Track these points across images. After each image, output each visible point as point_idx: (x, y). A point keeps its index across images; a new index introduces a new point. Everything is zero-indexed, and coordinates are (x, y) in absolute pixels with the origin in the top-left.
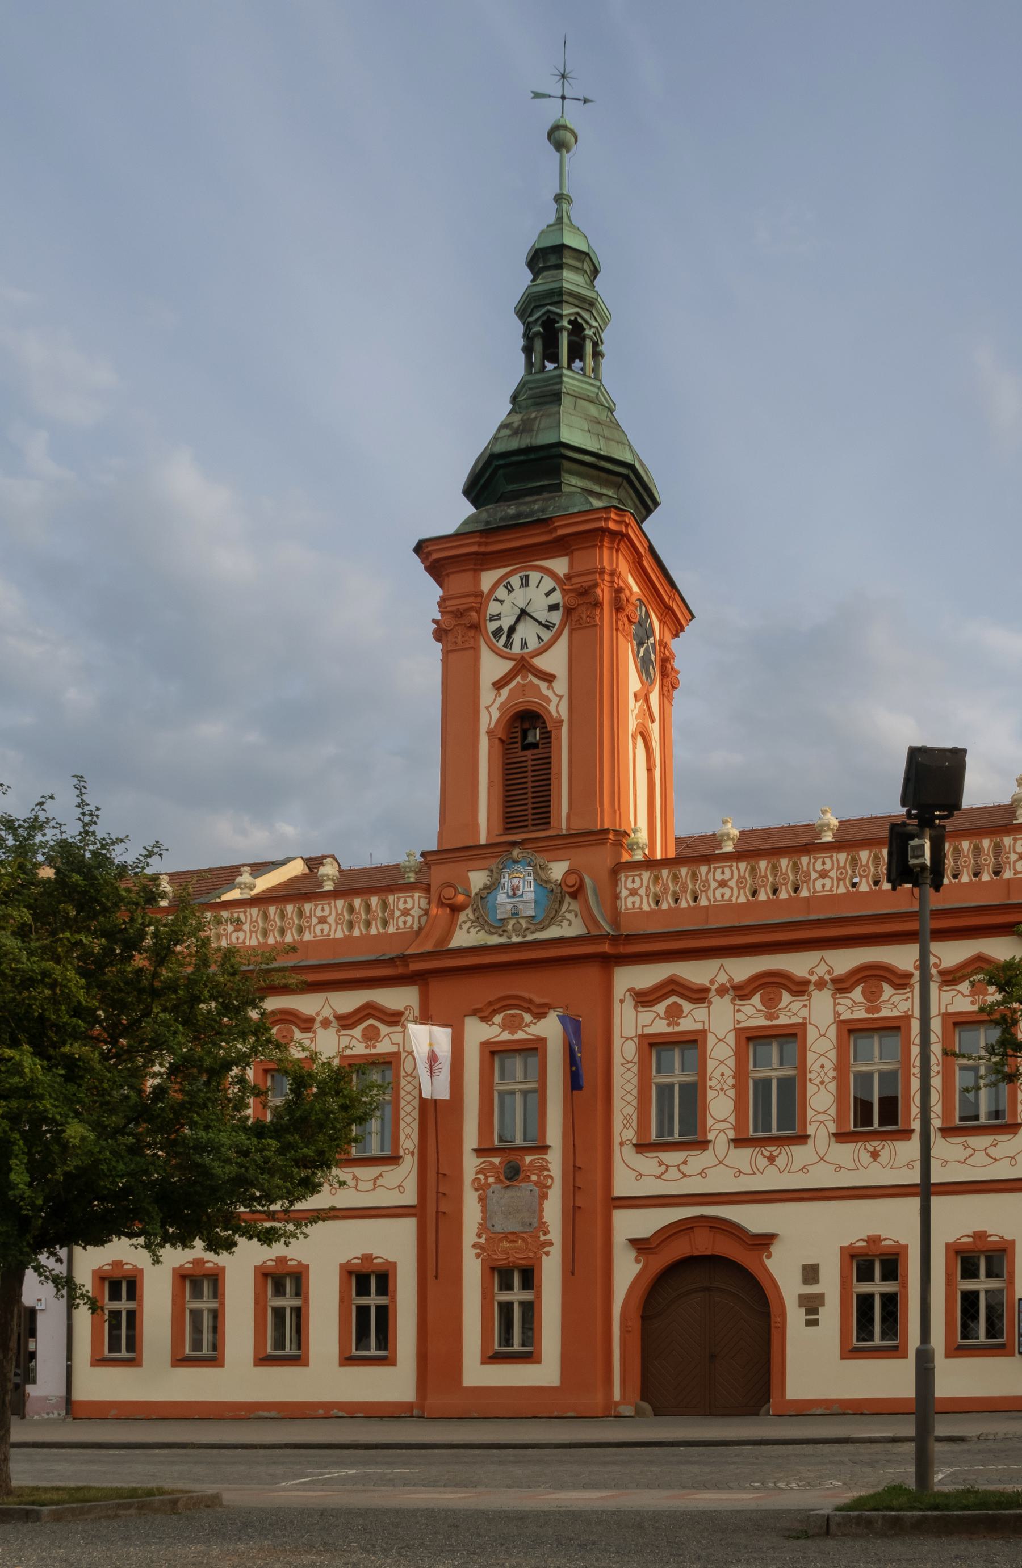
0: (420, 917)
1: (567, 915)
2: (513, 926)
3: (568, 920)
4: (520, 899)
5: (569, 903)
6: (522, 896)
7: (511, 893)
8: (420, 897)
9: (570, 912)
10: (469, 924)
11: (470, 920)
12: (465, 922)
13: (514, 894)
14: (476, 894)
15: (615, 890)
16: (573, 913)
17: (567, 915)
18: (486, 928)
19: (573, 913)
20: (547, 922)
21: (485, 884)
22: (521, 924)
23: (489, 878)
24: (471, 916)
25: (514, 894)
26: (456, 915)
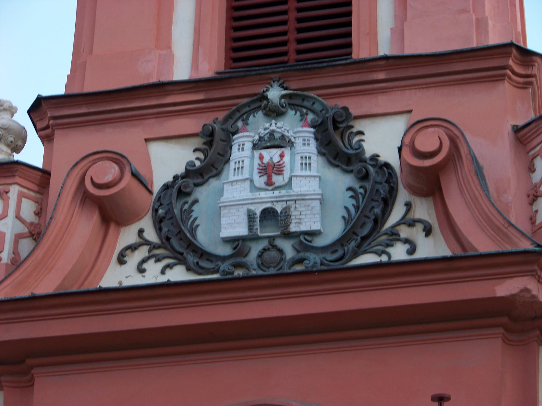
0: (18, 237)
1: (404, 232)
2: (260, 256)
3: (406, 241)
4: (283, 192)
5: (408, 205)
6: (289, 185)
7: (259, 181)
8: (21, 196)
9: (412, 224)
10: (143, 252)
11: (147, 243)
12: (133, 248)
13: (269, 183)
14: (166, 187)
15: (531, 178)
16: (419, 227)
17: (404, 232)
18: (191, 259)
19: (419, 227)
20: (353, 244)
21: (190, 164)
22: (281, 251)
23: (202, 156)
24: (151, 235)
25: (269, 183)
26: (112, 227)
